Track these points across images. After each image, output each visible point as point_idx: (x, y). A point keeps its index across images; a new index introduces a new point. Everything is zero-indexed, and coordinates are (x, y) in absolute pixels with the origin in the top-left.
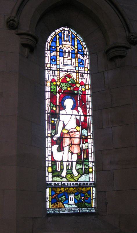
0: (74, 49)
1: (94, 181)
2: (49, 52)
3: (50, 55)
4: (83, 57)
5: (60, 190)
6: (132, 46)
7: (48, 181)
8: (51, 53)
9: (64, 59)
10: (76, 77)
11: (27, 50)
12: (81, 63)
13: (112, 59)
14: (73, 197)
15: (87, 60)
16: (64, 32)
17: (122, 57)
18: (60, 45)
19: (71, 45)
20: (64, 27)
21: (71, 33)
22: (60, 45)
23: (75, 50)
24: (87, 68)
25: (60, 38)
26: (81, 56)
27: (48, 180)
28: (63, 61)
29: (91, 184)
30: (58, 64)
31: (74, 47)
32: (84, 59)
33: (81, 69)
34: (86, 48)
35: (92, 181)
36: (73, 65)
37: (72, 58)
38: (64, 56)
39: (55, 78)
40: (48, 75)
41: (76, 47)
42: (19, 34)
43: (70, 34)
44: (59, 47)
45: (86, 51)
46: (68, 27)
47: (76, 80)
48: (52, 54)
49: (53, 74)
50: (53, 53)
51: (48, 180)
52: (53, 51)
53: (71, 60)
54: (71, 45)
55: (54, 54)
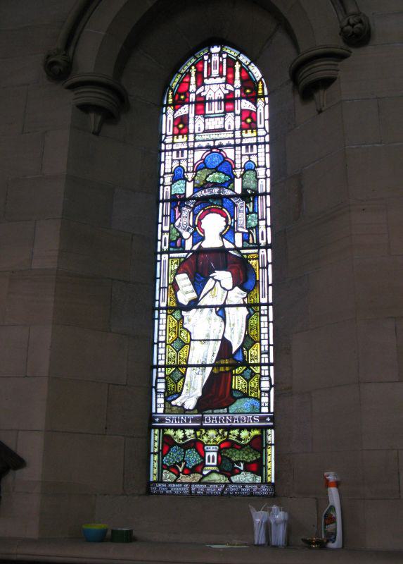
0: (232, 89)
1: (272, 410)
2: (170, 110)
3: (173, 115)
4: (255, 103)
5: (185, 436)
6: (352, 50)
7: (156, 413)
8: (175, 111)
9: (205, 118)
10: (235, 154)
11: (93, 119)
12: (249, 121)
13: (307, 93)
14: (215, 454)
15: (263, 110)
16: (210, 57)
17: (327, 82)
18: (197, 88)
19: (226, 83)
20: (211, 43)
21: (225, 56)
22: (197, 88)
23: (233, 92)
24: (264, 128)
25: (199, 74)
26: (251, 104)
27: (156, 410)
28: (204, 123)
29: (262, 419)
30: (191, 131)
31: (233, 85)
32: (257, 108)
33: (249, 136)
34: (263, 80)
35: (267, 411)
36: (227, 128)
37: (226, 112)
38: (207, 112)
39: (184, 164)
40: (168, 163)
41: (238, 83)
42: (72, 87)
43: (223, 59)
44: (195, 92)
45: (263, 89)
46: (222, 43)
47: (234, 162)
48: (177, 112)
49: (178, 156)
50: (179, 110)
51: (156, 410)
52: (182, 105)
53: (224, 117)
54: (226, 83)
55: (183, 111)
